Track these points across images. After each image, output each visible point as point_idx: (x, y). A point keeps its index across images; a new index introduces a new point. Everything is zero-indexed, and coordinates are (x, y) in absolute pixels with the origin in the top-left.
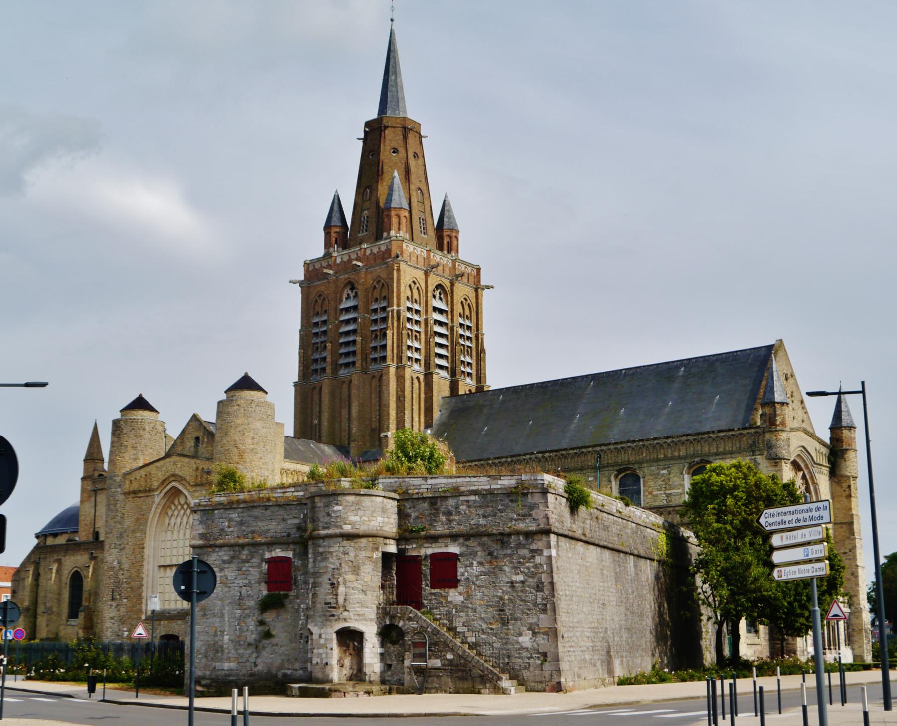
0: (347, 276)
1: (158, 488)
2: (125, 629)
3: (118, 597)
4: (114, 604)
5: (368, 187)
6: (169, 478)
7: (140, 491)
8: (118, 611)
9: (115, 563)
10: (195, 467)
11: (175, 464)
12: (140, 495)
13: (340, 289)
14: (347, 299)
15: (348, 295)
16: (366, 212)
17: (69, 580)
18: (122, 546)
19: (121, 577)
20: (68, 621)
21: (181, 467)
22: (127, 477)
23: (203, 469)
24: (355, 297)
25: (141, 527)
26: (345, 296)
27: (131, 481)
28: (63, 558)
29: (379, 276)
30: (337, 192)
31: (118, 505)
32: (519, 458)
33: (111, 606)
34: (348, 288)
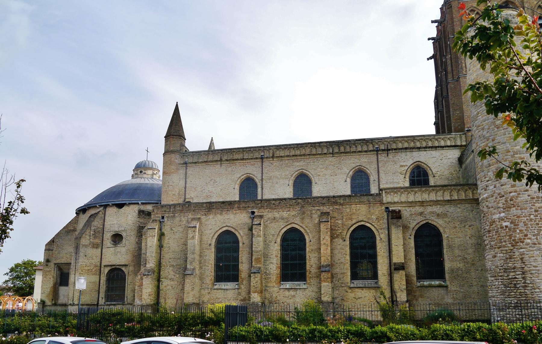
17: (214, 240)
20: (214, 285)
28: (203, 217)
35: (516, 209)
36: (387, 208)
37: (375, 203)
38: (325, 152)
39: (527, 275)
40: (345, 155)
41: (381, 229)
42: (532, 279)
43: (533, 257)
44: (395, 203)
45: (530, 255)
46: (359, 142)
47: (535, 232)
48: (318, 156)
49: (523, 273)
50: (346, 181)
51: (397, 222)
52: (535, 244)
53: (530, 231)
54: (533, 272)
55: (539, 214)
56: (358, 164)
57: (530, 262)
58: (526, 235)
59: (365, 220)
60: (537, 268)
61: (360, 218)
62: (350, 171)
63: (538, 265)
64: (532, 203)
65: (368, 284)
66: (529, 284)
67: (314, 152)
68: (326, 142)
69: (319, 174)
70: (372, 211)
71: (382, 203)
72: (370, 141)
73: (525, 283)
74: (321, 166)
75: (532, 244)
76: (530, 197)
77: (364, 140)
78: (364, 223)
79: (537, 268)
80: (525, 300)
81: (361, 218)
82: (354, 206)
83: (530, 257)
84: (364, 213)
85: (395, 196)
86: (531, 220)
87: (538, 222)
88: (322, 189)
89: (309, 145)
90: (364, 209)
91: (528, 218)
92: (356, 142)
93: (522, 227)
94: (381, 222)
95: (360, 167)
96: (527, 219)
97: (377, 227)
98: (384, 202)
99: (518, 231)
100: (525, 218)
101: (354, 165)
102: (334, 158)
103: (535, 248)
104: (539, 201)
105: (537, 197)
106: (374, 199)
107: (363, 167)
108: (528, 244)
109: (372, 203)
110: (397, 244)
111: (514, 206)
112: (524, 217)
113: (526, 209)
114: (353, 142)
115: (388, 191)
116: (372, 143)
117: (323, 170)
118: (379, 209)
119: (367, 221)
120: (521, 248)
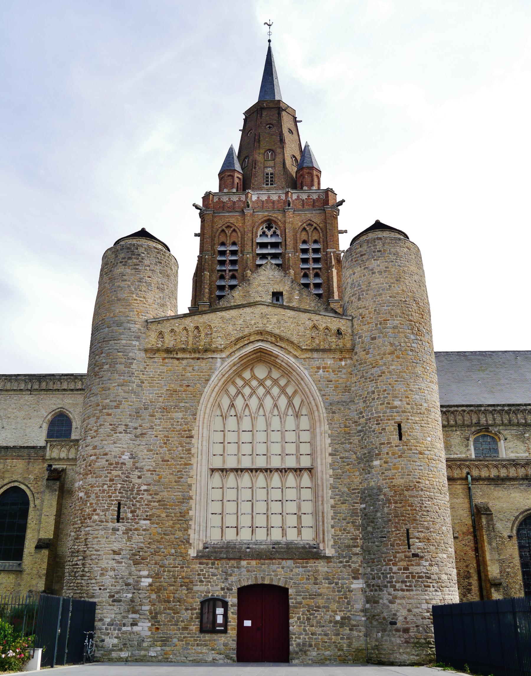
0: (266, 214)
1: (225, 348)
2: (145, 573)
3: (130, 515)
4: (121, 526)
5: (270, 150)
6: (250, 335)
7: (184, 350)
8: (129, 539)
9: (126, 457)
10: (310, 324)
11: (263, 316)
12: (180, 355)
13: (257, 224)
14: (261, 236)
15: (264, 233)
16: (270, 169)
18: (139, 432)
19: (136, 481)
21: (279, 322)
22: (153, 327)
23: (327, 328)
24: (271, 236)
25: (182, 404)
26: (260, 232)
27: (161, 333)
29: (309, 220)
30: (232, 145)
31: (134, 366)
32: (518, 408)
33: (115, 530)
34: (264, 227)
35: (92, 477)
36: (50, 466)
37: (36, 458)
38: (22, 388)
39: (86, 561)
40: (45, 393)
41: (38, 493)
42: (91, 566)
43: (97, 538)
44: (60, 459)
45: (94, 535)
46: (65, 377)
47: (104, 507)
48: (12, 393)
49: (84, 559)
50: (41, 427)
51: (54, 484)
52: (102, 522)
53: (100, 505)
54: (93, 557)
55: (114, 484)
56: (60, 406)
57: (93, 545)
58: (95, 510)
59: (20, 480)
60: (98, 553)
61: (14, 477)
62: (48, 414)
63: (101, 549)
64: (108, 470)
65: (10, 565)
66: (87, 572)
67: (8, 386)
68: (25, 375)
69: (9, 415)
70: (31, 468)
71: (44, 459)
72: (80, 377)
73: (83, 571)
74: (13, 406)
75: (99, 521)
76: (107, 463)
77: (72, 375)
78: (18, 483)
79: (98, 553)
80: (80, 593)
81: (15, 478)
82: (10, 460)
83: (93, 538)
84: (20, 471)
85: (62, 450)
86: (104, 491)
87: (110, 494)
88: (9, 436)
89: (3, 378)
90: (21, 465)
91: (101, 488)
92: (62, 377)
93: (93, 499)
94: (40, 483)
95: (62, 409)
96: (100, 490)
97: (33, 490)
98: (47, 457)
99: (88, 504)
100: (98, 489)
101: (55, 407)
102: (31, 396)
103: (101, 527)
104: (117, 467)
105: (116, 463)
106: (35, 453)
107: (65, 410)
108: (94, 522)
109: (32, 458)
110: (48, 514)
111: (91, 473)
112: (97, 487)
113: (101, 477)
114: (58, 377)
115: (54, 444)
116: (81, 380)
117: (15, 411)
118: (40, 466)
119: (22, 481)
120: (88, 527)
